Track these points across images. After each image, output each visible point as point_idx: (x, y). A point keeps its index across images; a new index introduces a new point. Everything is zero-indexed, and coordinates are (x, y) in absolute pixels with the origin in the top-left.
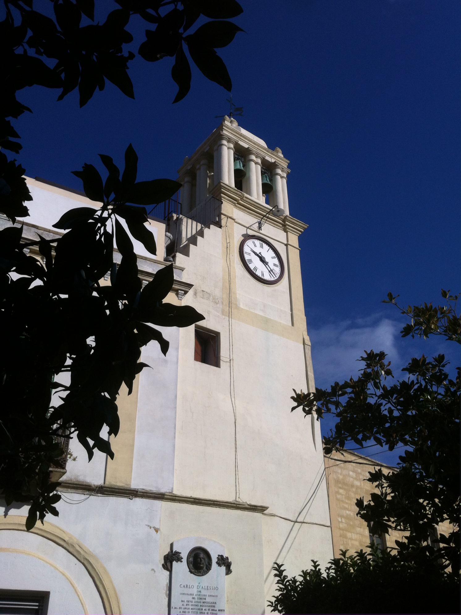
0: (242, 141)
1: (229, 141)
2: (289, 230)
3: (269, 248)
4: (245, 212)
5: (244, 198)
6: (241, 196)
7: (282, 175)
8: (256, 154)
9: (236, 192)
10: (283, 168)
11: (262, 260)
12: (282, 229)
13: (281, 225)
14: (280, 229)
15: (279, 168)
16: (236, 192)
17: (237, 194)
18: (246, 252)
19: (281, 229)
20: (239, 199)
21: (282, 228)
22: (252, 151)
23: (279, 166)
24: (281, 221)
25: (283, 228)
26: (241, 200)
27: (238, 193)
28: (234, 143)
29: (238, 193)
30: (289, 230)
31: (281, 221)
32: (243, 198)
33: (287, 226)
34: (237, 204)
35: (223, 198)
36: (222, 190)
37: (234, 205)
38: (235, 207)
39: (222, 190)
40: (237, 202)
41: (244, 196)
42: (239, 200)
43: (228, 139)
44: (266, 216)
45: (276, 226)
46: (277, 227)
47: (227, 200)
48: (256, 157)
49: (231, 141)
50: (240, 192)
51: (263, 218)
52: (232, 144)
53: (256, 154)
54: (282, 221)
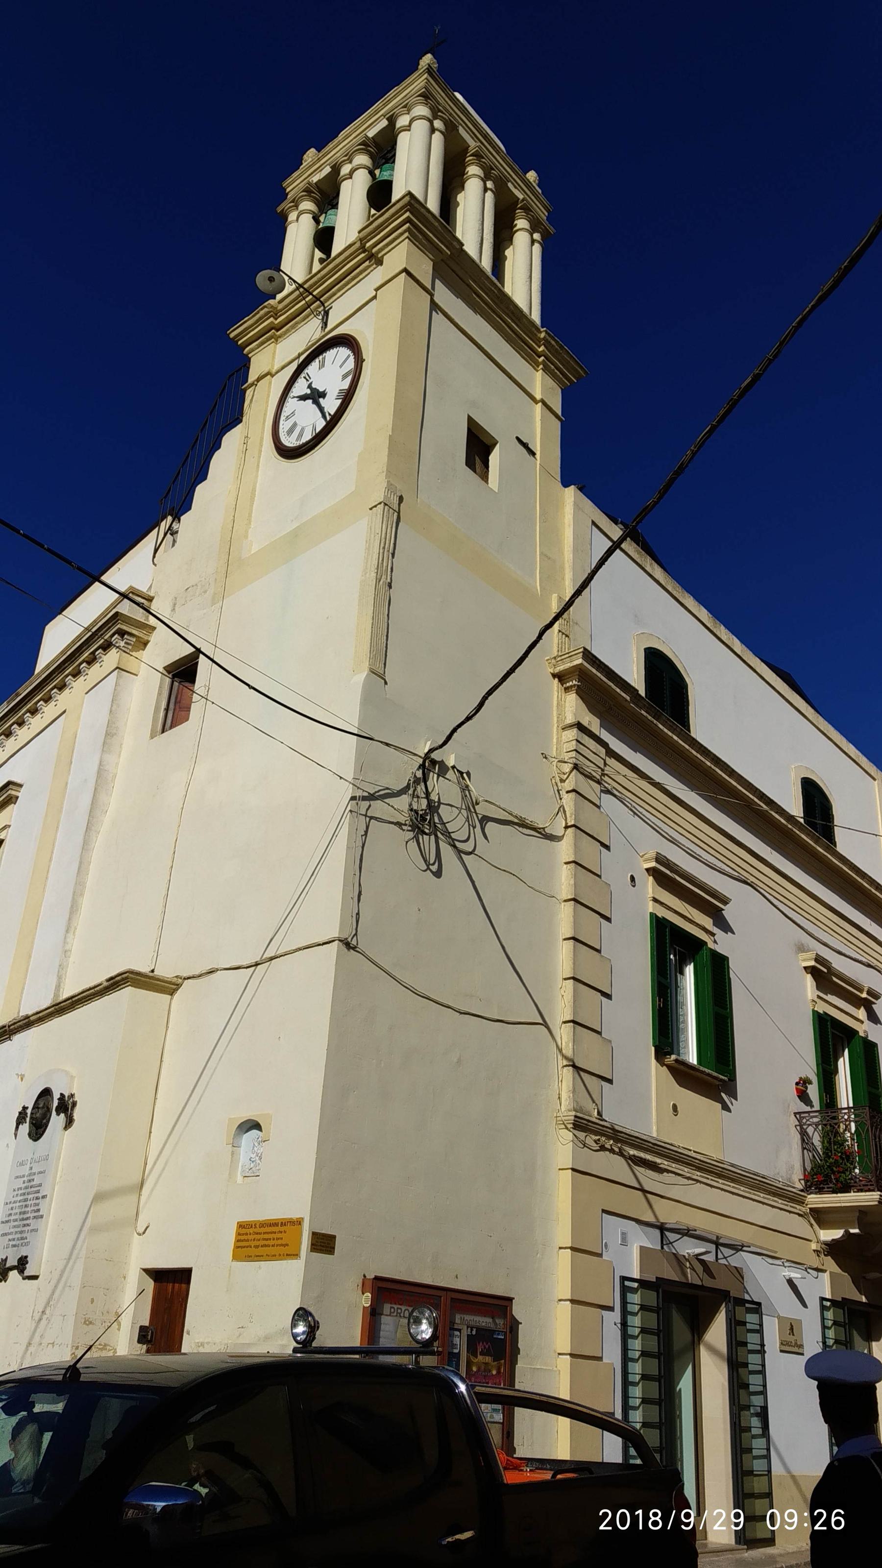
0: (323, 167)
1: (296, 204)
2: (383, 253)
3: (338, 348)
4: (299, 326)
5: (280, 307)
6: (269, 312)
7: (407, 123)
8: (346, 156)
9: (258, 316)
10: (405, 107)
11: (315, 396)
12: (375, 266)
13: (367, 263)
14: (372, 271)
15: (398, 116)
16: (258, 316)
17: (260, 318)
18: (287, 417)
19: (372, 268)
20: (272, 319)
21: (372, 265)
22: (337, 162)
23: (395, 113)
24: (363, 255)
25: (374, 260)
26: (276, 319)
27: (262, 312)
28: (302, 196)
29: (262, 312)
30: (383, 253)
31: (363, 255)
32: (276, 308)
33: (374, 250)
34: (278, 330)
35: (250, 353)
36: (240, 342)
37: (273, 340)
38: (280, 340)
39: (240, 342)
40: (273, 331)
41: (272, 307)
42: (272, 322)
43: (292, 204)
44: (318, 296)
45: (361, 277)
46: (364, 275)
47: (258, 348)
48: (351, 162)
49: (297, 201)
50: (262, 309)
51: (321, 302)
52: (302, 201)
53: (346, 156)
54: (364, 252)
